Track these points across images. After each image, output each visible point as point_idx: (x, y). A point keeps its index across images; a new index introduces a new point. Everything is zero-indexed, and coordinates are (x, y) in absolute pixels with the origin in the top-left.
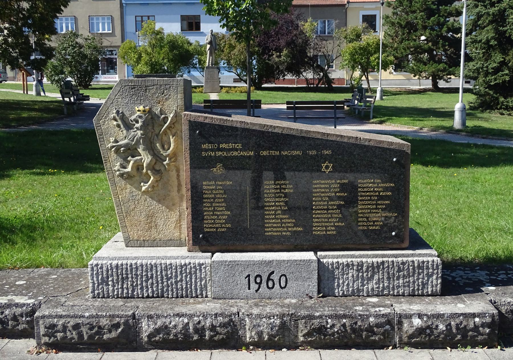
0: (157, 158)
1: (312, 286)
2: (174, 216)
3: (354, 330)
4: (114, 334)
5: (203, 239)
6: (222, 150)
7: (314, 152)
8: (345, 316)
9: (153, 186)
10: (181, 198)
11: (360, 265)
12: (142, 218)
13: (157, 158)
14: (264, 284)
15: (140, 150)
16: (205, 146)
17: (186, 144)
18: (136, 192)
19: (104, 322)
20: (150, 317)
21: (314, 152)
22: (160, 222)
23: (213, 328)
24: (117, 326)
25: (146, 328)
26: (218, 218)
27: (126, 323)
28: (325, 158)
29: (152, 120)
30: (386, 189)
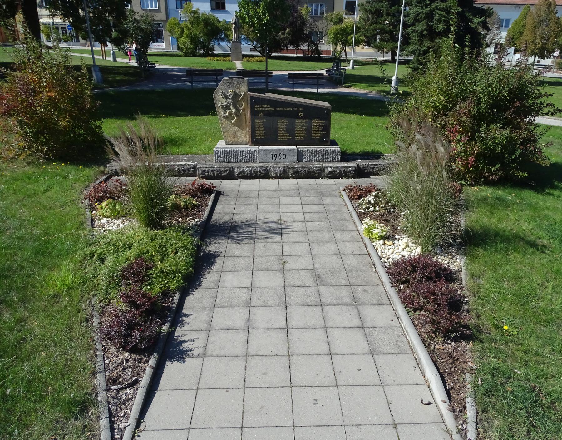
0: (238, 110)
1: (295, 158)
2: (244, 133)
3: (308, 172)
4: (225, 174)
5: (255, 142)
6: (262, 108)
8: (305, 167)
9: (236, 121)
10: (247, 126)
11: (312, 151)
12: (232, 133)
13: (238, 110)
14: (277, 158)
16: (256, 106)
17: (249, 105)
19: (222, 169)
20: (238, 168)
22: (239, 135)
23: (260, 171)
24: (227, 170)
25: (237, 171)
26: (260, 134)
27: (230, 170)
28: (300, 111)
29: (236, 96)
30: (322, 123)
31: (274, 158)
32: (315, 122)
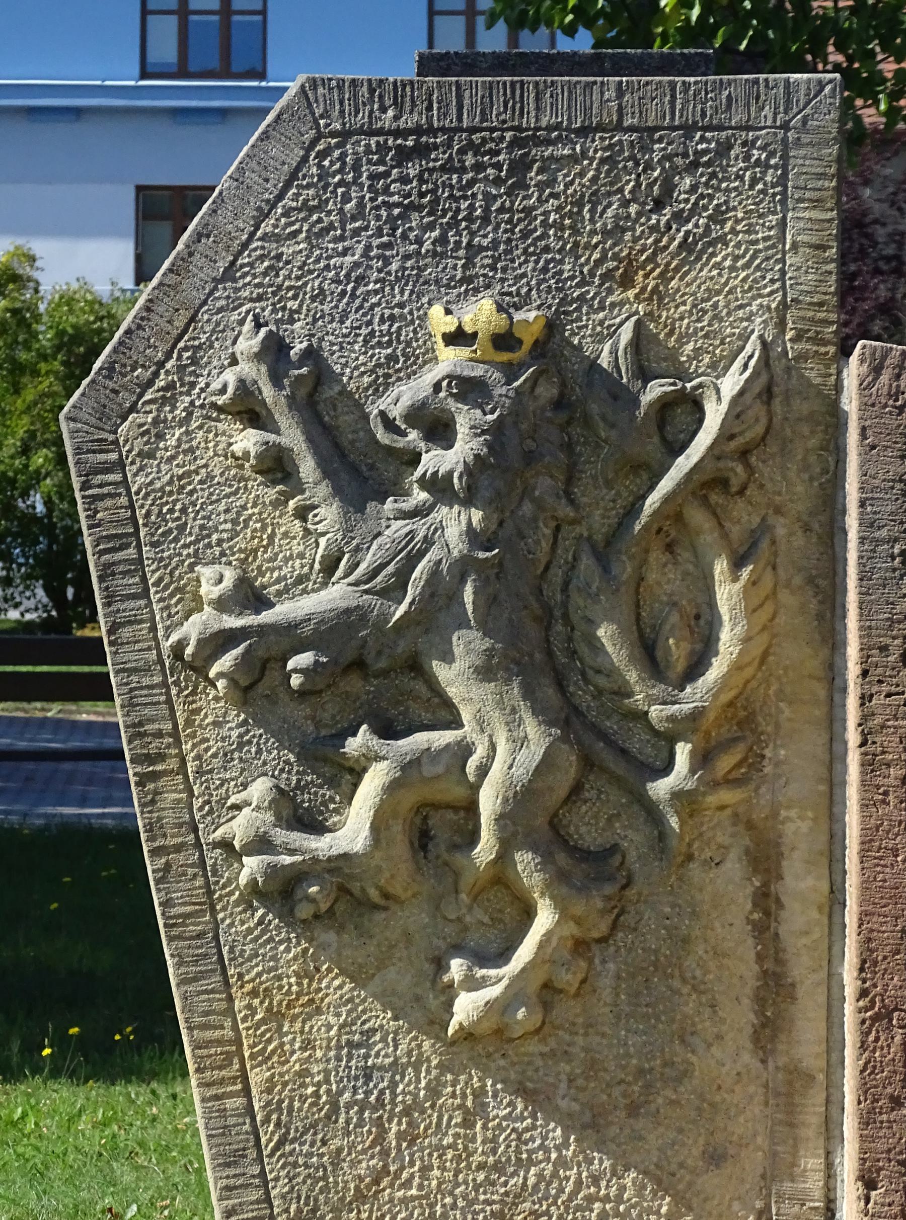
0: (599, 745)
9: (542, 990)
13: (599, 745)
15: (453, 676)
18: (397, 1041)
29: (565, 426)
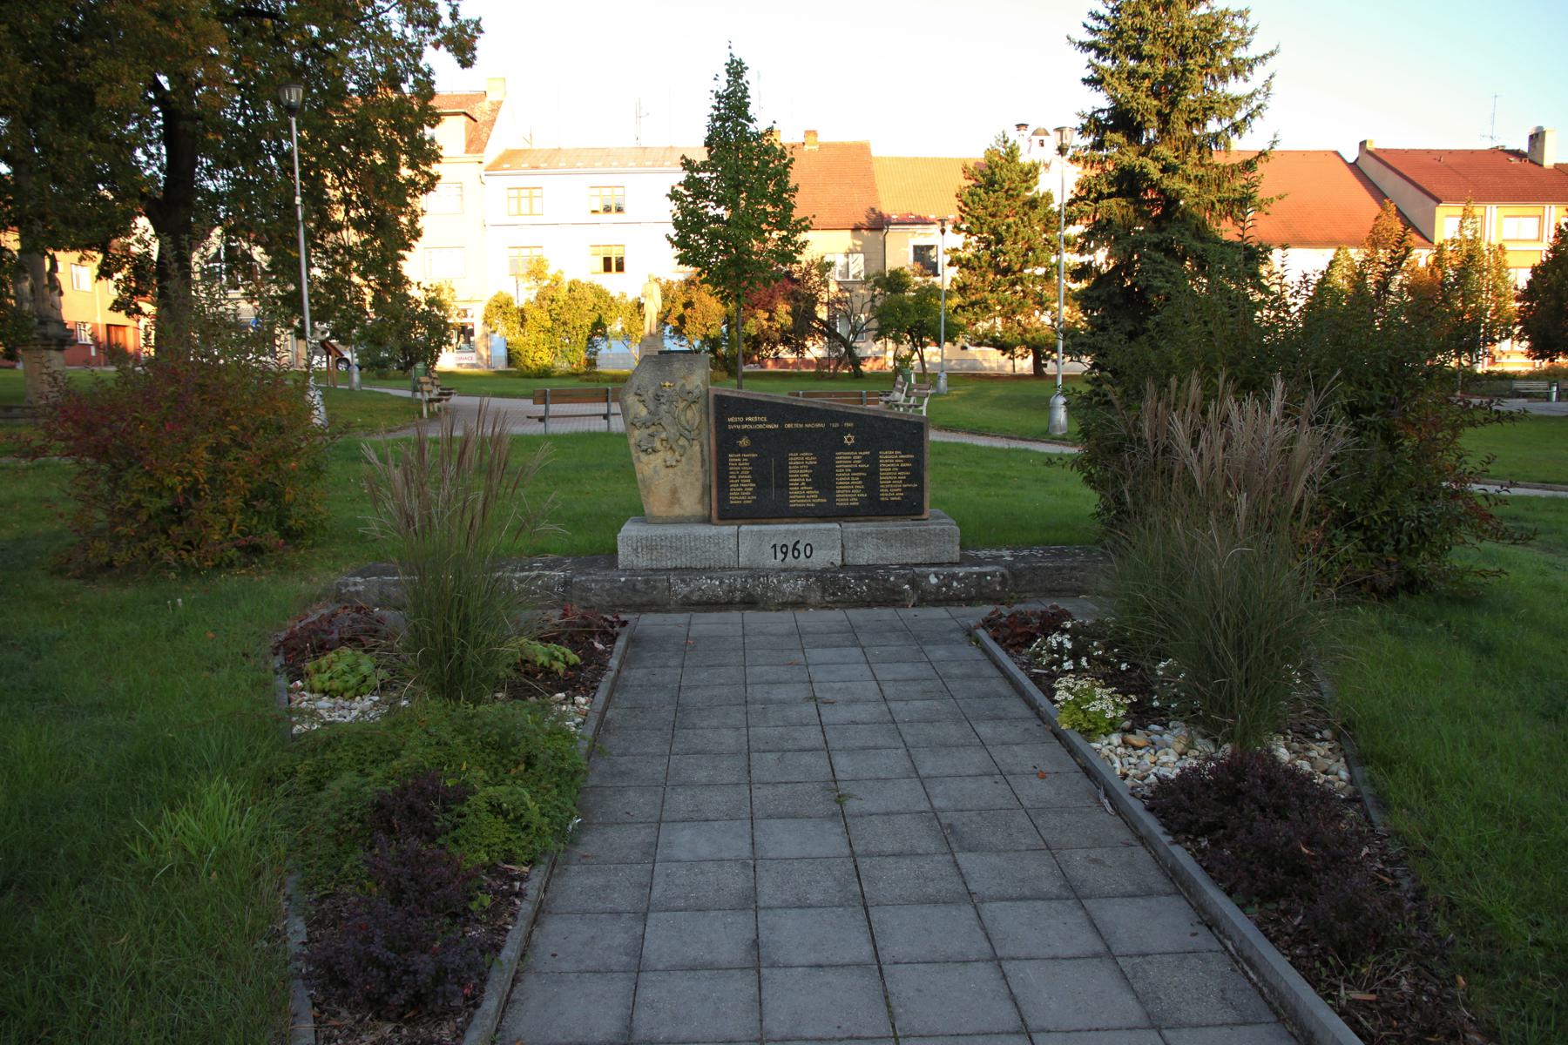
5: (728, 513)
7: (836, 425)
16: (731, 420)
21: (836, 425)
28: (848, 431)
30: (906, 461)
31: (780, 556)
32: (889, 459)
